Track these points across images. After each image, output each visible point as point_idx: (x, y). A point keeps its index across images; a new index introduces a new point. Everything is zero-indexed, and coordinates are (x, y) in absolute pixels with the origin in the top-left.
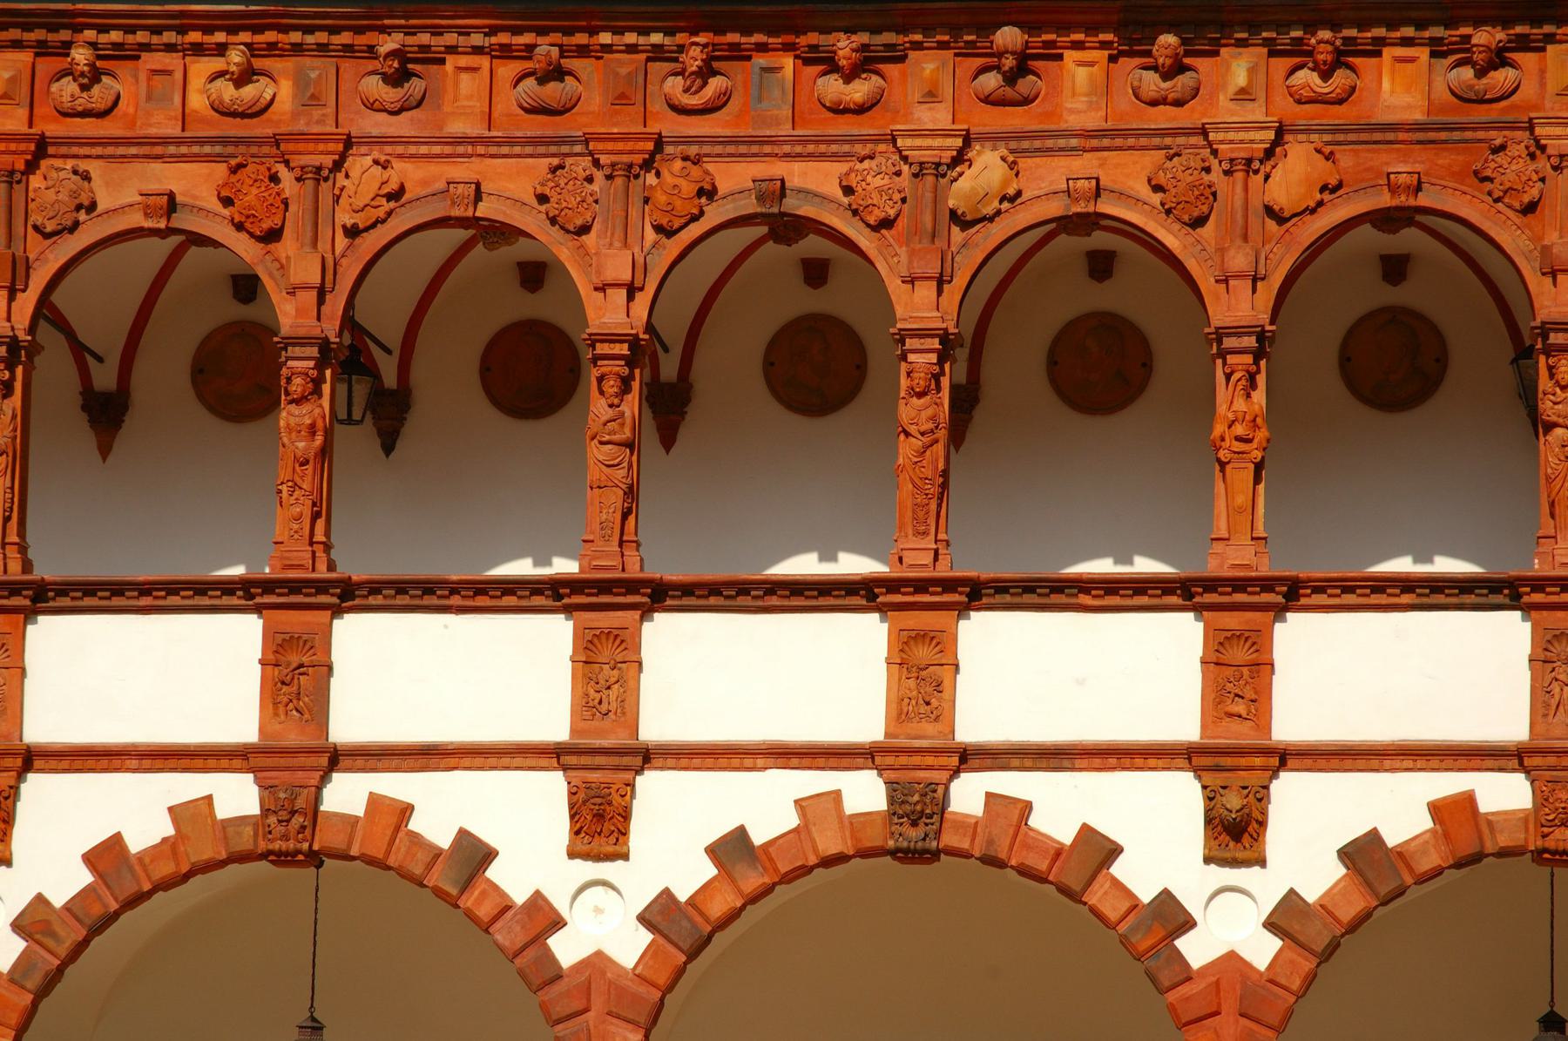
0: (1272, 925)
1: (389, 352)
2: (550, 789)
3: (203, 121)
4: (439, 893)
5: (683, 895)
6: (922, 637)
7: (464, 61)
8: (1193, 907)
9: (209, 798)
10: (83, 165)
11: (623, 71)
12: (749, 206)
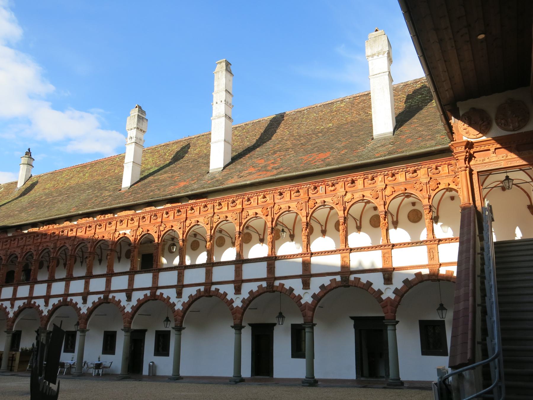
0: (394, 293)
1: (291, 230)
2: (300, 281)
3: (260, 204)
4: (288, 295)
5: (317, 294)
6: (345, 257)
7: (287, 192)
8: (383, 291)
9: (262, 285)
10: (247, 211)
11: (305, 190)
12: (321, 204)
